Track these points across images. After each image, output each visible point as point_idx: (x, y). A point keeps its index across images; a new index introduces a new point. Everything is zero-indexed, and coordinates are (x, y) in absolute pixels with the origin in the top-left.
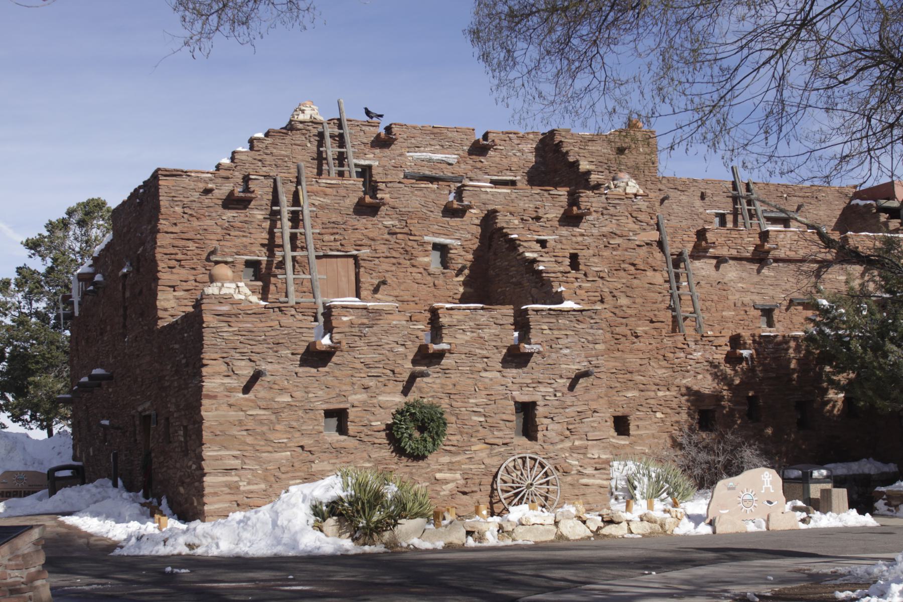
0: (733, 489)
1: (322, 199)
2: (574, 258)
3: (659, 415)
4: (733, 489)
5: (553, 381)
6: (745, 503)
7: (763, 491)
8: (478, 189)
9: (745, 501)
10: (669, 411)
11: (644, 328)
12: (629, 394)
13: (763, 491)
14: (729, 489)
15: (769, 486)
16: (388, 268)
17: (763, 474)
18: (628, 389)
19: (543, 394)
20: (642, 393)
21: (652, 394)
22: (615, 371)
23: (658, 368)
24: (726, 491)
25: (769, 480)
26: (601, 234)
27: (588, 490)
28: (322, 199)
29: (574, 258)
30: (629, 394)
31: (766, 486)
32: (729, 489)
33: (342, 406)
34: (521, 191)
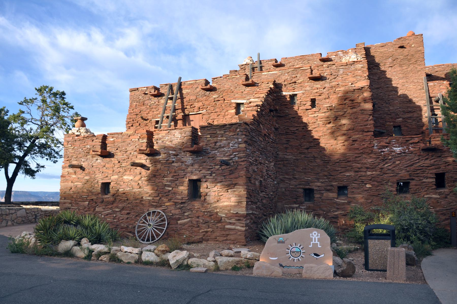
0: (283, 242)
1: (187, 91)
2: (313, 101)
3: (368, 186)
4: (283, 242)
5: (211, 167)
6: (292, 254)
7: (311, 246)
8: (261, 74)
9: (293, 252)
10: (376, 183)
11: (358, 136)
12: (348, 174)
13: (311, 246)
14: (279, 242)
15: (317, 242)
16: (216, 118)
17: (312, 233)
18: (347, 171)
19: (205, 175)
20: (357, 173)
21: (363, 174)
22: (338, 161)
23: (369, 158)
24: (276, 244)
25: (317, 238)
26: (330, 86)
27: (231, 233)
28: (187, 91)
29: (313, 101)
30: (348, 174)
31: (313, 242)
32: (279, 242)
33: (108, 181)
34: (284, 71)
